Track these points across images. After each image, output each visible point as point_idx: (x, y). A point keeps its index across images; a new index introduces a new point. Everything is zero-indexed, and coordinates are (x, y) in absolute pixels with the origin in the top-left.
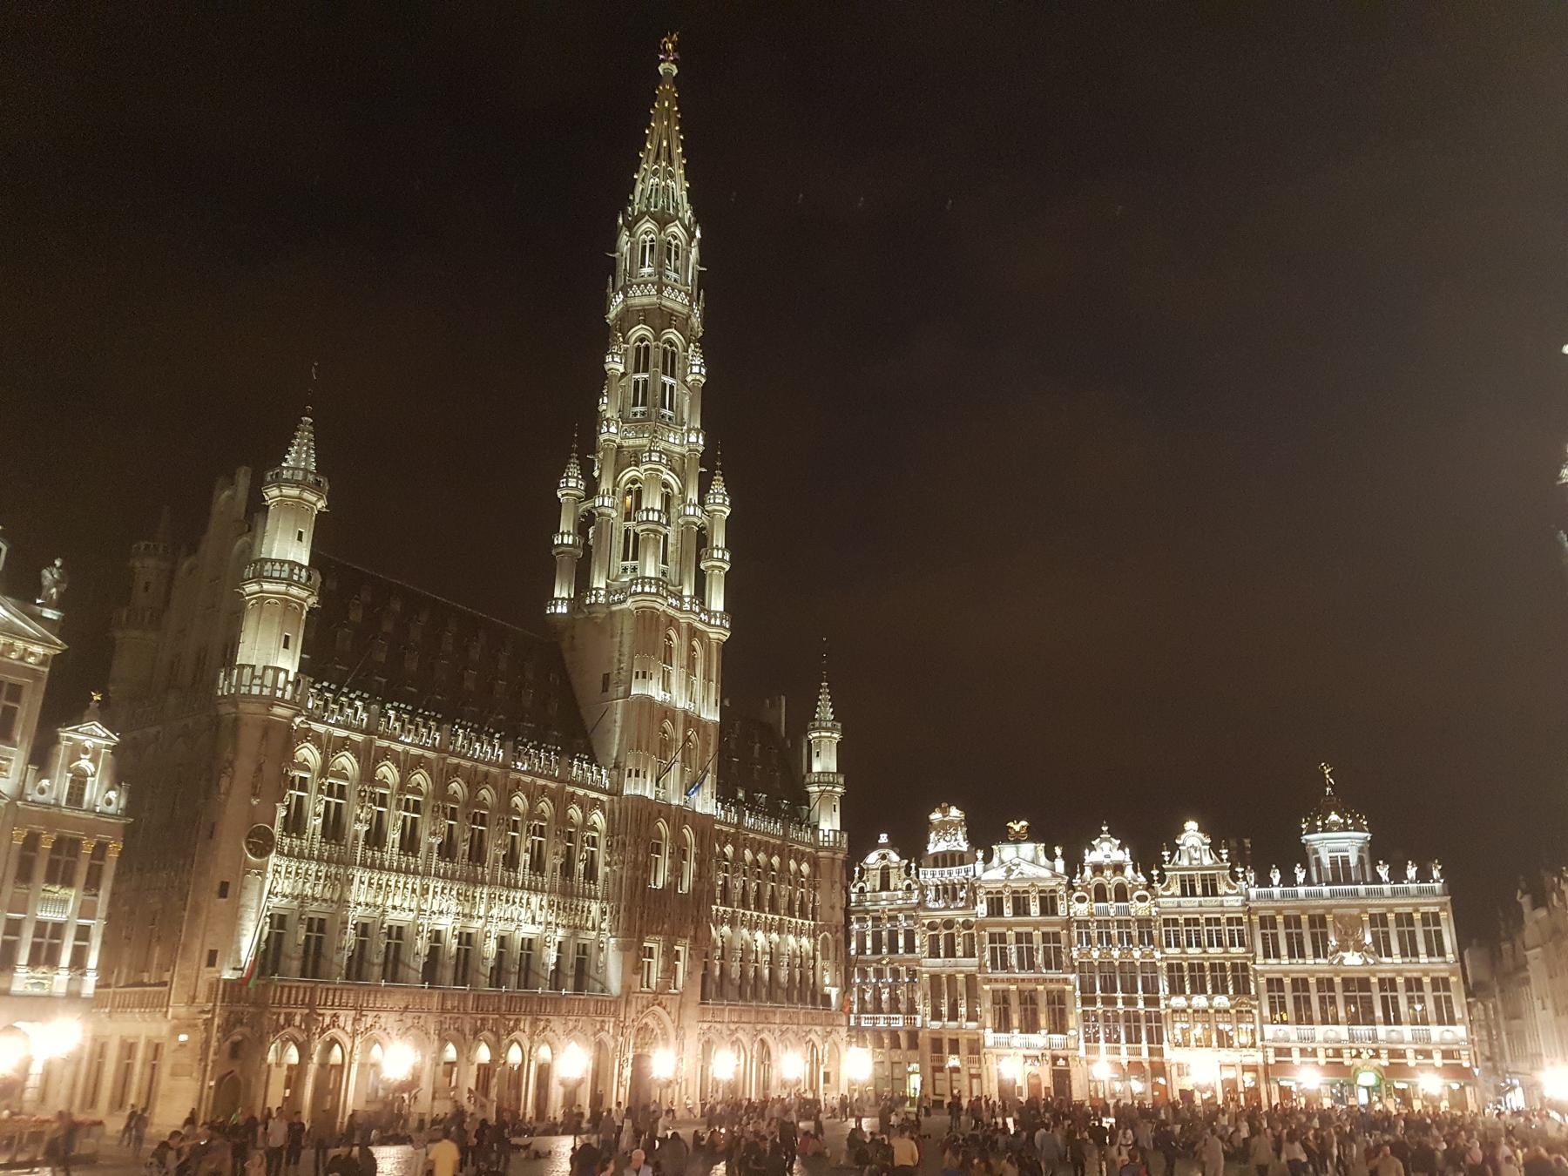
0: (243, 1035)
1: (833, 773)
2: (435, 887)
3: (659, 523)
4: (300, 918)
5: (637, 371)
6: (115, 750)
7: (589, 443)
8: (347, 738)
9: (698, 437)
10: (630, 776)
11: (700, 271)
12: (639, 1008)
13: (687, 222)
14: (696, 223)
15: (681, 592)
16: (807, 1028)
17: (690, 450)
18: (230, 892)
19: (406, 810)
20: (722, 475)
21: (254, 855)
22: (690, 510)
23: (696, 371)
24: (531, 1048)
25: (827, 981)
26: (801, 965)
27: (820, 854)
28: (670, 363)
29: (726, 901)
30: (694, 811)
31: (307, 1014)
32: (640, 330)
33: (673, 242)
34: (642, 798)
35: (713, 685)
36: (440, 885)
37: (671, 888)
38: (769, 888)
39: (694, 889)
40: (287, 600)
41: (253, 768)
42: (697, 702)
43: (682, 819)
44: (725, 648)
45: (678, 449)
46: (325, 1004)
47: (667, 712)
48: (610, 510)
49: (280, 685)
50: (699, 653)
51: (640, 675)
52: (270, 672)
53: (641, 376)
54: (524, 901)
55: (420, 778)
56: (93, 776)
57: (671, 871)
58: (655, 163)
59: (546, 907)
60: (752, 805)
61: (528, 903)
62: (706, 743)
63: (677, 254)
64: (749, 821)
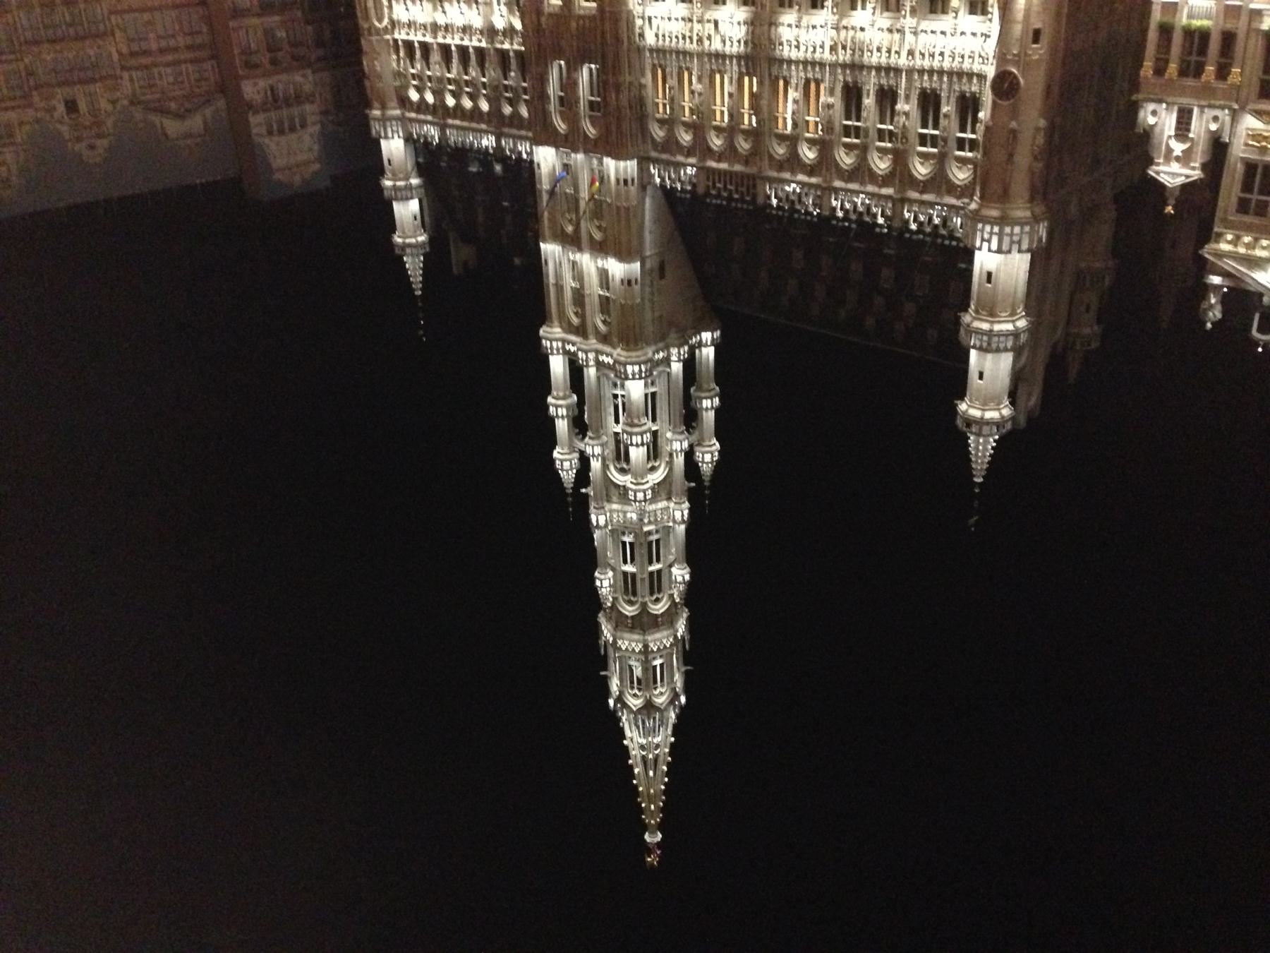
1: (396, 199)
3: (631, 434)
4: (956, 13)
5: (659, 572)
6: (1150, 161)
7: (694, 497)
8: (922, 192)
9: (597, 521)
10: (633, 180)
13: (625, 711)
14: (615, 711)
17: (603, 508)
18: (1031, 35)
19: (857, 128)
21: (1011, 73)
23: (605, 582)
28: (628, 585)
29: (503, 55)
30: (557, 147)
32: (659, 608)
34: (617, 157)
35: (552, 280)
36: (817, 56)
37: (573, 66)
38: (454, 71)
39: (547, 66)
42: (566, 261)
43: (570, 139)
44: (542, 317)
45: (615, 506)
47: (600, 248)
48: (674, 438)
49: (995, 240)
50: (570, 311)
52: (1005, 248)
53: (655, 567)
54: (728, 43)
55: (846, 160)
56: (1170, 137)
57: (575, 84)
58: (657, 755)
60: (484, 156)
61: (724, 42)
62: (552, 220)
63: (632, 682)
64: (488, 142)
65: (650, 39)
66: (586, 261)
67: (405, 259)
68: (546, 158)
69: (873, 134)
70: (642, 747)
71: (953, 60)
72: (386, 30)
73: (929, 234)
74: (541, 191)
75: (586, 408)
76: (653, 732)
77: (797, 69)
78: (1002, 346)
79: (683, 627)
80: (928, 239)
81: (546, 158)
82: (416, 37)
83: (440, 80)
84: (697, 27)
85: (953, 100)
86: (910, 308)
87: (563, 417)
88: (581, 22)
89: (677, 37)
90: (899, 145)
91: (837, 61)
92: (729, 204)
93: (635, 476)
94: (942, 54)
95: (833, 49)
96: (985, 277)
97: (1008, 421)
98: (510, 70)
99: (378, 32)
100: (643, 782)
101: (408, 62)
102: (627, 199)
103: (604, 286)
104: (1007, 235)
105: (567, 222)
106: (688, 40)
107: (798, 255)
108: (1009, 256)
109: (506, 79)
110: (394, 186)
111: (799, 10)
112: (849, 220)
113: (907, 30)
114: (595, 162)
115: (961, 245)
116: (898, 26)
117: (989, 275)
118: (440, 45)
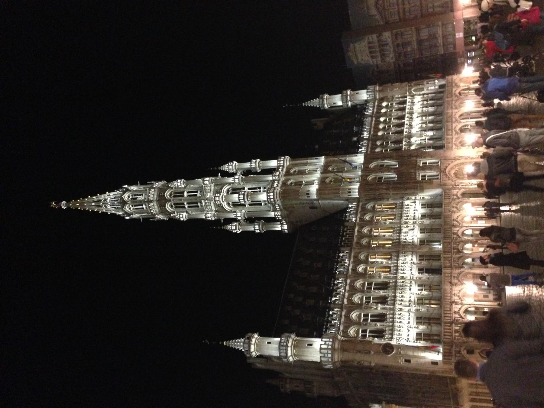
0: (464, 350)
1: (342, 96)
2: (401, 273)
3: (244, 195)
5: (184, 207)
7: (217, 221)
8: (345, 316)
9: (206, 180)
10: (350, 195)
11: (140, 184)
12: (447, 179)
14: (122, 188)
15: (271, 180)
16: (454, 95)
17: (212, 183)
19: (371, 288)
20: (220, 167)
21: (393, 351)
22: (237, 180)
23: (180, 184)
24: (465, 227)
25: (433, 88)
26: (427, 100)
27: (378, 97)
28: (179, 194)
29: (401, 142)
30: (363, 164)
31: (455, 324)
32: (168, 207)
33: (131, 197)
34: (360, 189)
35: (309, 161)
36: (400, 271)
37: (396, 171)
39: (396, 160)
40: (294, 347)
41: (359, 354)
42: (317, 167)
45: (213, 188)
46: (450, 317)
47: (322, 182)
48: (242, 213)
50: (296, 169)
51: (309, 196)
52: (322, 351)
53: (186, 206)
54: (405, 234)
55: (358, 284)
57: (389, 171)
59: (407, 225)
61: (406, 233)
63: (135, 195)
64: (366, 135)
65: (407, 202)
66: (317, 176)
67: (318, 99)
68: (359, 159)
70: (105, 200)
71: (398, 327)
72: (410, 93)
73: (328, 319)
74: (346, 157)
75: (255, 175)
76: (113, 205)
78: (282, 351)
79: (160, 218)
80: (326, 319)
81: (359, 159)
82: (408, 105)
83: (391, 115)
84: (411, 222)
85: (382, 327)
86: (298, 312)
87: (251, 165)
88: (413, 174)
89: (407, 213)
91: (398, 279)
92: (340, 236)
93: (226, 197)
95: (403, 278)
96: (310, 343)
97: (250, 355)
99: (410, 89)
100: (89, 200)
101: (398, 102)
102: (342, 193)
103: (306, 183)
104: (328, 352)
105: (333, 168)
106: (406, 218)
107: (320, 265)
108: (319, 353)
110: (348, 95)
111: (418, 263)
112: (333, 287)
113: (410, 308)
114: (358, 179)
115: (323, 333)
116: (411, 304)
117: (311, 345)
118: (405, 115)
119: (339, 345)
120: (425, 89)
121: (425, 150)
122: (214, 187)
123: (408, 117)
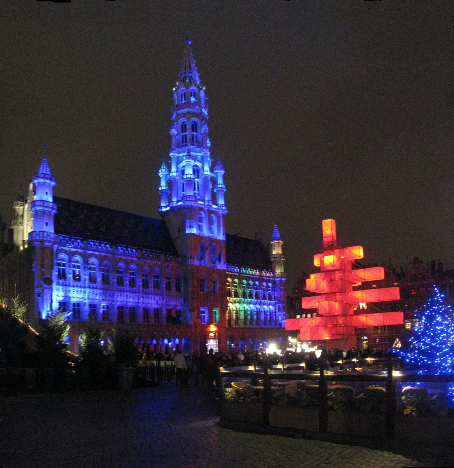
1: (280, 254)
10: (188, 258)
15: (204, 199)
25: (280, 319)
27: (276, 280)
61: (154, 298)
66: (205, 232)
69: (97, 269)
72: (278, 303)
77: (127, 290)
80: (73, 237)
81: (222, 266)
82: (267, 301)
83: (260, 289)
85: (68, 278)
87: (220, 184)
88: (206, 305)
90: (86, 266)
93: (190, 165)
94: (74, 292)
96: (49, 224)
98: (234, 292)
101: (271, 294)
106: (168, 299)
108: (40, 230)
109: (236, 289)
110: (280, 258)
111: (127, 306)
113: (87, 299)
114: (203, 264)
116: (90, 300)
119: (48, 245)
120: (279, 313)
121: (228, 313)
122: (200, 156)
123: (257, 301)
